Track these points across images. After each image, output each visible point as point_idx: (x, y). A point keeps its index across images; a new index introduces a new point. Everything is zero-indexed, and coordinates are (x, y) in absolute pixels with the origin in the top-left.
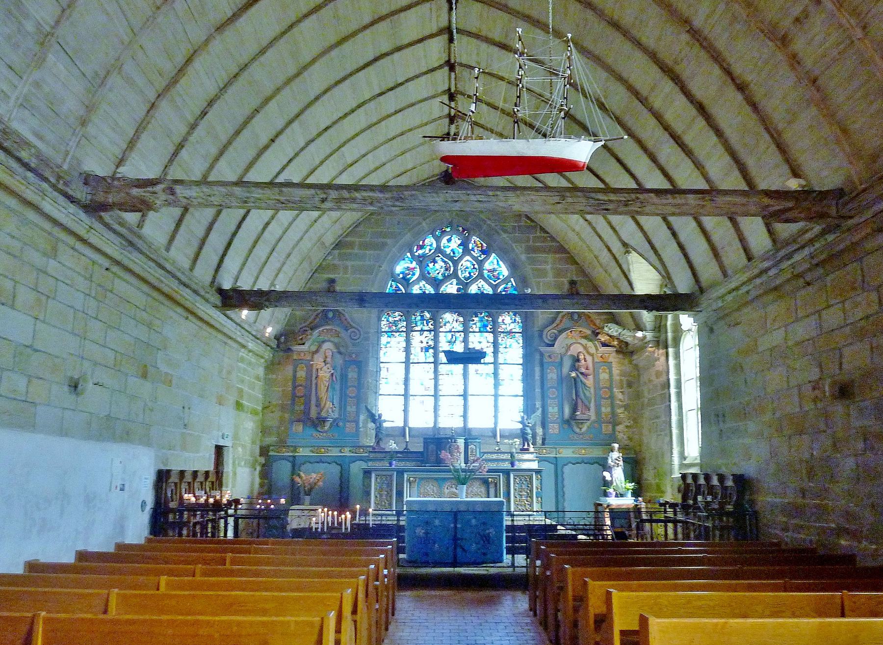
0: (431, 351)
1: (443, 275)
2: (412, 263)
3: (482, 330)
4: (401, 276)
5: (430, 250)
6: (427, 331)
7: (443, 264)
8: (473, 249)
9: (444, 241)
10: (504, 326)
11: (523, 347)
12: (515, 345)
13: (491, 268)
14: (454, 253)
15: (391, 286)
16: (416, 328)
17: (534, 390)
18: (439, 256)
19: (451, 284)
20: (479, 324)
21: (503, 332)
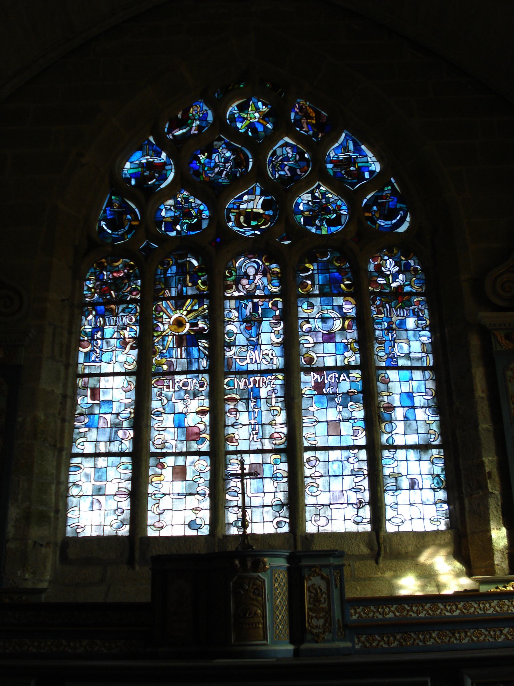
0: (203, 343)
1: (231, 176)
2: (159, 155)
3: (327, 290)
4: (133, 182)
5: (200, 128)
6: (192, 297)
7: (228, 154)
8: (298, 123)
9: (233, 109)
10: (382, 281)
11: (432, 328)
12: (411, 322)
13: (342, 157)
14: (254, 130)
15: (110, 204)
16: (167, 293)
17: (476, 426)
18: (220, 139)
19: (251, 192)
20: (320, 278)
21: (380, 294)
